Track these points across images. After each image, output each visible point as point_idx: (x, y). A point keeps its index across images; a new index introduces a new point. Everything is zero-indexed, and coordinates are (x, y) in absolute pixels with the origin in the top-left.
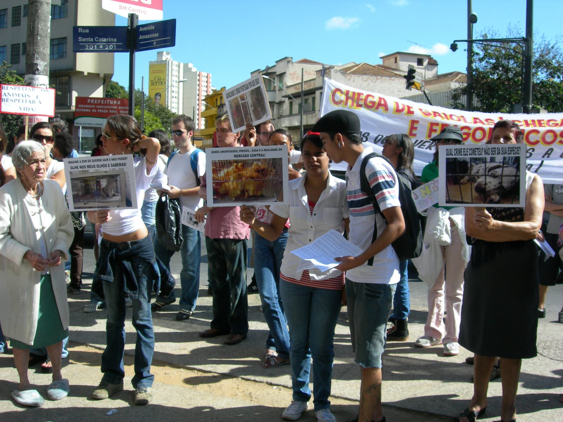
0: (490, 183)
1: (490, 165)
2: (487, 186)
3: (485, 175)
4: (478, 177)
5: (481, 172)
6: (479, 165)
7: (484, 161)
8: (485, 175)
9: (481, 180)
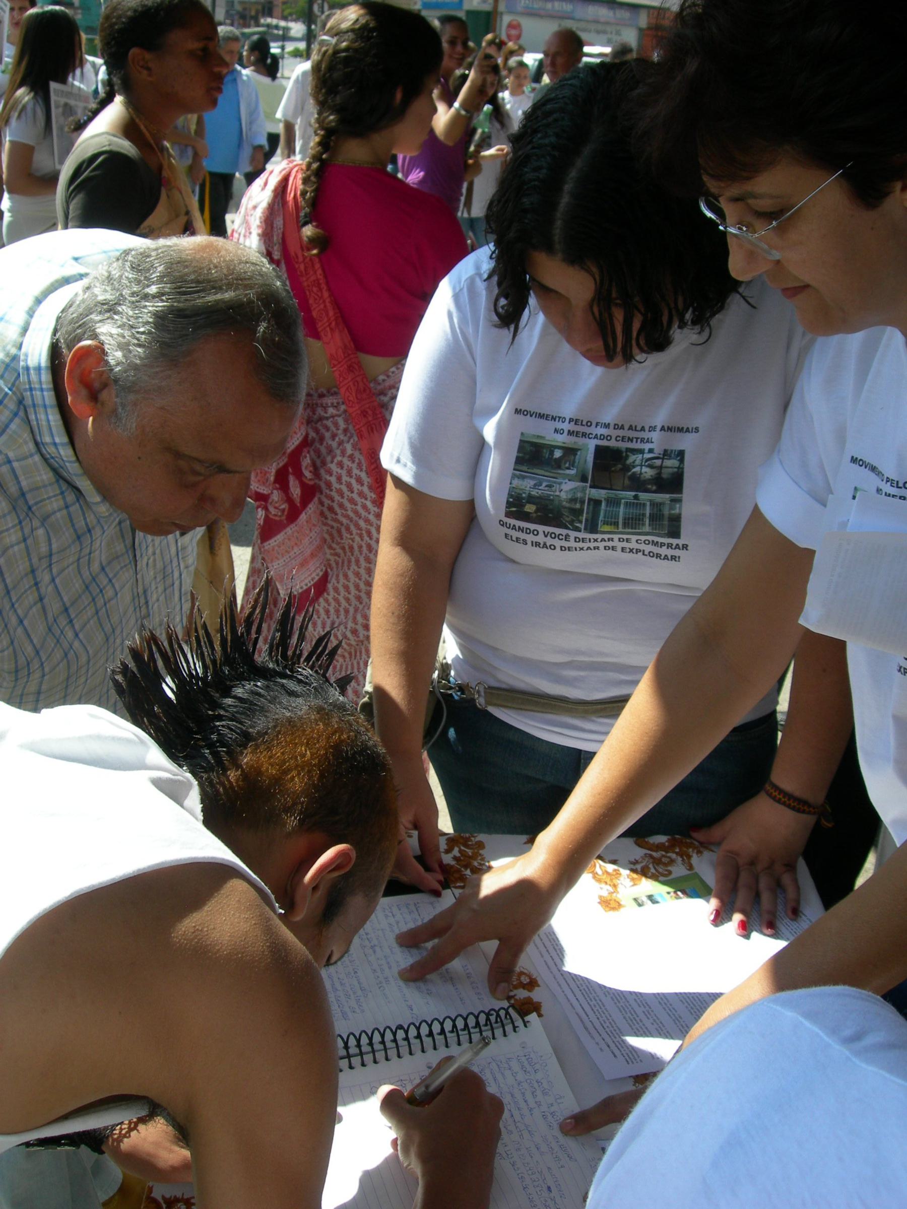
0: (646, 472)
1: (647, 456)
2: (642, 476)
3: (641, 466)
4: (634, 467)
5: (638, 462)
6: (636, 456)
7: (641, 451)
8: (641, 466)
9: (637, 469)
